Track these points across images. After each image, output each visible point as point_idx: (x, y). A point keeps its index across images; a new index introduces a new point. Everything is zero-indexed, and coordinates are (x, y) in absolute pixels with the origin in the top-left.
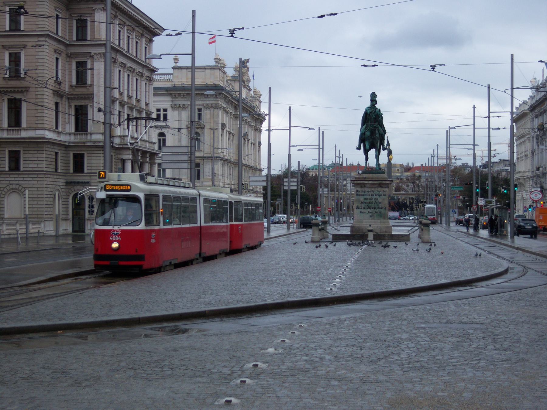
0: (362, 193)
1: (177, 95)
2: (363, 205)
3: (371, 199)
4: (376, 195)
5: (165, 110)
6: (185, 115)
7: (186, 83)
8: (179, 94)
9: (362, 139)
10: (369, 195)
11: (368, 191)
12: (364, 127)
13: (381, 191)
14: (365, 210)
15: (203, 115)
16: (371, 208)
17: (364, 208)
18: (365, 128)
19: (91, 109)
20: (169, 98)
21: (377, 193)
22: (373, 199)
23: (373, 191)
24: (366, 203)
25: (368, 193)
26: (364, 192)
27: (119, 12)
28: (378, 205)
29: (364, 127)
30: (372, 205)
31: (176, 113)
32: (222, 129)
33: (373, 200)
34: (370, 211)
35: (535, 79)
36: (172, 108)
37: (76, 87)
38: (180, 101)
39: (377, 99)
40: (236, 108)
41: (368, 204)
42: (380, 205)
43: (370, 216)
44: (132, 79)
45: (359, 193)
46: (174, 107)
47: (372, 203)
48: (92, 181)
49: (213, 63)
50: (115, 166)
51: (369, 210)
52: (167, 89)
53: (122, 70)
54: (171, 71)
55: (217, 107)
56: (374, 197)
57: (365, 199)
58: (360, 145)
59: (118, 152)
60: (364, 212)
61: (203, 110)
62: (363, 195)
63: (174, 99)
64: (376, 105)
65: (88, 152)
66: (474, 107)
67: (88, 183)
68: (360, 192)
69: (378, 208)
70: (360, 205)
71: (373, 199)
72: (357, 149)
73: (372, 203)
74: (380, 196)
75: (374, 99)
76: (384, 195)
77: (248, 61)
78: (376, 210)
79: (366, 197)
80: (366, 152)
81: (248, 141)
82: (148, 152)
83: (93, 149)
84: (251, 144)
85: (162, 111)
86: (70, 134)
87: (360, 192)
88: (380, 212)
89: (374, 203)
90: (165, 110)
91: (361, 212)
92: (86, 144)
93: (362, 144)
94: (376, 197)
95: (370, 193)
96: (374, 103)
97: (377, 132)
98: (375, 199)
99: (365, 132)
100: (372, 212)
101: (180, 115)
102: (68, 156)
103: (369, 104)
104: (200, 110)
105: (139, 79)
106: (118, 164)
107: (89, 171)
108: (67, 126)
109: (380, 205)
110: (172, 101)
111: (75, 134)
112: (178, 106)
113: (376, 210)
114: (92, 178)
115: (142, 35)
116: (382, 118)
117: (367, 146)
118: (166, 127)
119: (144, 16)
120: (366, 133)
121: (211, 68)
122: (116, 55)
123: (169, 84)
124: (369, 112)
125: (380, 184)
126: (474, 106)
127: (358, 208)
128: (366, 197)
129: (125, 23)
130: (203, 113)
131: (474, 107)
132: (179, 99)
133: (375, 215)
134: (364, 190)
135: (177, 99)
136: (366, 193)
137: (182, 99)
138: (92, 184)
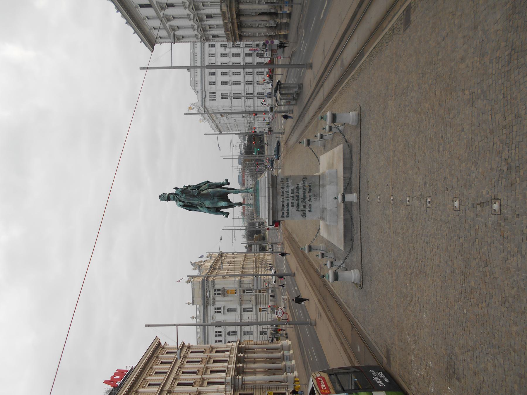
0: (285, 209)
1: (207, 303)
2: (301, 208)
4: (287, 192)
5: (215, 309)
6: (218, 298)
7: (165, 388)
8: (207, 302)
9: (217, 210)
10: (288, 200)
11: (283, 202)
12: (199, 208)
14: (307, 207)
15: (217, 289)
17: (304, 206)
18: (201, 207)
20: (209, 307)
21: (285, 190)
26: (283, 207)
27: (134, 388)
29: (199, 208)
31: (217, 303)
32: (225, 278)
34: (308, 199)
36: (214, 305)
38: (211, 301)
40: (215, 269)
41: (300, 202)
43: (315, 199)
44: (186, 368)
45: (285, 214)
46: (214, 304)
47: (298, 197)
49: (191, 283)
50: (248, 390)
52: (204, 309)
53: (177, 382)
54: (195, 306)
55: (213, 282)
56: (290, 194)
57: (293, 205)
58: (223, 213)
59: (237, 388)
60: (310, 207)
61: (215, 289)
62: (288, 208)
63: (210, 304)
66: (206, 134)
68: (283, 213)
70: (301, 213)
71: (292, 195)
72: (227, 217)
74: (288, 187)
75: (166, 196)
77: (191, 262)
80: (231, 205)
81: (231, 261)
82: (237, 356)
84: (233, 259)
85: (215, 311)
87: (283, 213)
89: (297, 194)
90: (215, 309)
93: (221, 210)
95: (285, 199)
96: (171, 196)
100: (310, 196)
101: (218, 301)
103: (173, 203)
104: (215, 290)
105: (187, 360)
106: (246, 387)
109: (301, 185)
110: (210, 305)
112: (213, 302)
113: (308, 191)
115: (157, 357)
116: (189, 186)
117: (223, 204)
118: (224, 308)
119: (142, 360)
120: (206, 206)
121: (193, 285)
122: (165, 391)
123: (202, 308)
124: (181, 203)
126: (205, 134)
127: (304, 215)
129: (144, 379)
130: (216, 289)
131: (206, 134)
132: (209, 301)
135: (210, 303)
137: (210, 300)
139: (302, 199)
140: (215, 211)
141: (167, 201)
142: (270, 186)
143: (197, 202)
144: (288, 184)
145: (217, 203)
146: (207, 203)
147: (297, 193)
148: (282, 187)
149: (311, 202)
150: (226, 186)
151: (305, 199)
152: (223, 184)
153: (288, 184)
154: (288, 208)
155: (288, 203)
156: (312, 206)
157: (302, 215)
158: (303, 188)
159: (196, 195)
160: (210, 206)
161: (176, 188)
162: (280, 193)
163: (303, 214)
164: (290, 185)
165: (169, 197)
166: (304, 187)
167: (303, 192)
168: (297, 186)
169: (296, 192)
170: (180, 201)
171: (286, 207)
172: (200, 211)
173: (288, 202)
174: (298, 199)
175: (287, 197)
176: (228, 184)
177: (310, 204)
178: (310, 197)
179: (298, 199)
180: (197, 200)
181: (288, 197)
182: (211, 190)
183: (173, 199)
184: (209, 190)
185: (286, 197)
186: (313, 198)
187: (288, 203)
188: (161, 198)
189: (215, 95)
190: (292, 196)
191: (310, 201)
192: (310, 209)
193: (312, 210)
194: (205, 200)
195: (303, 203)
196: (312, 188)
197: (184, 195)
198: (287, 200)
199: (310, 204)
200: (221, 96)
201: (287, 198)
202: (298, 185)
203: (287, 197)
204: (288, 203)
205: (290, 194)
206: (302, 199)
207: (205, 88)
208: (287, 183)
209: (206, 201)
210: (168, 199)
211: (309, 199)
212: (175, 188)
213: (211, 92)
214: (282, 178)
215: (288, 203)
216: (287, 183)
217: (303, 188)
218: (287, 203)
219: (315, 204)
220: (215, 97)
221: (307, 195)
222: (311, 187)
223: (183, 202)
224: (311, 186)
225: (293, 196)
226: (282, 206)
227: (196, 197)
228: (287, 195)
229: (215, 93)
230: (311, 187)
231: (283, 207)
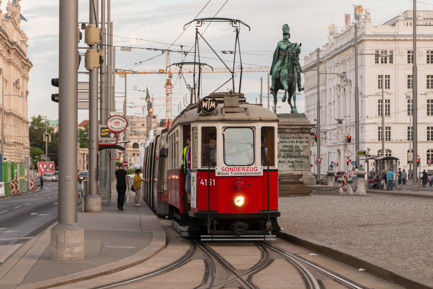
4: (297, 142)
10: (289, 142)
11: (288, 138)
12: (279, 63)
13: (302, 138)
14: (284, 159)
16: (291, 157)
21: (298, 140)
22: (294, 146)
23: (294, 138)
24: (285, 151)
25: (287, 140)
28: (300, 154)
29: (279, 63)
30: (293, 154)
35: (333, 25)
39: (290, 32)
43: (290, 167)
47: (292, 151)
51: (289, 159)
56: (294, 145)
60: (284, 162)
64: (289, 39)
69: (299, 157)
71: (294, 146)
73: (292, 151)
74: (301, 143)
75: (288, 32)
76: (306, 142)
78: (297, 160)
79: (285, 144)
88: (301, 162)
89: (294, 151)
95: (290, 140)
96: (287, 36)
97: (295, 70)
98: (296, 147)
99: (280, 70)
100: (293, 162)
103: (281, 38)
109: (302, 153)
113: (297, 160)
120: (283, 71)
125: (301, 129)
128: (285, 144)
133: (296, 165)
134: (282, 136)
136: (286, 140)
140: (276, 77)
141: (282, 32)
142: (302, 127)
143: (287, 62)
144: (303, 143)
145: (285, 79)
146: (285, 71)
147: (296, 151)
149: (288, 163)
150: (297, 88)
151: (290, 157)
152: (299, 85)
153: (303, 143)
155: (287, 142)
156: (284, 164)
158: (300, 156)
159: (295, 62)
160: (282, 75)
161: (301, 45)
162: (296, 136)
164: (303, 144)
165: (287, 35)
170: (288, 47)
171: (284, 141)
172: (274, 63)
173: (288, 142)
174: (290, 151)
175: (292, 142)
176: (300, 90)
178: (292, 162)
179: (290, 151)
180: (288, 63)
182: (296, 75)
183: (285, 38)
184: (296, 73)
185: (292, 141)
186: (291, 164)
187: (287, 143)
188: (285, 26)
189: (386, 62)
193: (280, 164)
194: (288, 69)
197: (295, 52)
200: (384, 74)
203: (292, 142)
204: (287, 143)
205: (294, 145)
207: (400, 42)
208: (304, 142)
209: (287, 70)
210: (285, 34)
212: (301, 45)
213: (394, 54)
215: (287, 142)
216: (304, 142)
217: (300, 156)
220: (382, 62)
221: (293, 159)
223: (287, 49)
227: (292, 62)
229: (391, 62)
231: (284, 138)
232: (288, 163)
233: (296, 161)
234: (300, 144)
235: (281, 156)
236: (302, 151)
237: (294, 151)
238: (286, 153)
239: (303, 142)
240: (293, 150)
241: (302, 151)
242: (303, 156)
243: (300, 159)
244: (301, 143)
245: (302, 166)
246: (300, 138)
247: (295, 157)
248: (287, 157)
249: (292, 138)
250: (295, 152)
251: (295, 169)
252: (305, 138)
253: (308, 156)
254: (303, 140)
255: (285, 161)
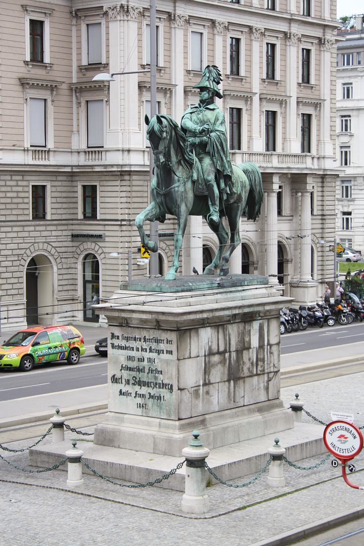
0: (123, 343)
2: (126, 374)
3: (141, 360)
4: (151, 351)
10: (138, 350)
11: (135, 339)
16: (140, 383)
17: (128, 382)
19: (108, 107)
21: (154, 346)
24: (130, 369)
28: (156, 378)
30: (144, 377)
33: (146, 363)
37: (85, 69)
41: (134, 373)
42: (161, 377)
43: (140, 406)
48: (107, 233)
51: (137, 388)
56: (147, 355)
57: (130, 358)
60: (127, 394)
62: (125, 348)
65: (102, 183)
67: (100, 236)
70: (118, 376)
71: (146, 360)
74: (159, 352)
78: (150, 390)
83: (107, 178)
86: (79, 152)
88: (159, 398)
89: (147, 371)
91: (121, 393)
92: (94, 170)
94: (153, 355)
98: (150, 360)
100: (143, 396)
102: (75, 189)
107: (103, 217)
108: (75, 139)
111: (85, 152)
113: (153, 392)
114: (107, 228)
133: (150, 402)
138: (107, 239)
139: (140, 378)
148: (158, 340)
149: (135, 397)
151: (140, 385)
153: (163, 353)
154: (126, 349)
157: (114, 376)
158: (156, 384)
163: (116, 379)
166: (157, 386)
167: (151, 382)
168: (159, 371)
169: (150, 368)
173: (135, 349)
174: (139, 370)
177: (131, 393)
178: (143, 395)
179: (139, 370)
181: (142, 351)
185: (142, 348)
190: (144, 359)
191: (136, 394)
192: (124, 392)
193: (122, 396)
195: (134, 380)
196: (156, 400)
198: (138, 348)
199: (131, 393)
201: (140, 350)
202: (161, 374)
204: (133, 350)
206: (140, 378)
208: (165, 352)
211: (140, 393)
214: (172, 341)
216: (165, 352)
218: (133, 348)
219: (131, 404)
221: (144, 390)
222: (158, 399)
224: (159, 401)
225: (144, 361)
226: (129, 337)
228: (146, 349)
230: (158, 399)
231: (127, 339)
232: (135, 397)
233: (150, 393)
234: (157, 354)
235: (124, 381)
236: (161, 371)
237: (147, 371)
238: (131, 373)
239: (163, 351)
240: (144, 368)
241: (161, 374)
242: (163, 384)
243: (158, 390)
244: (159, 355)
245: (160, 407)
246: (158, 341)
247: (147, 384)
248: (134, 384)
249: (143, 340)
250: (148, 373)
251: (146, 413)
252: (165, 342)
253: (172, 386)
254: (162, 346)
255: (130, 392)
